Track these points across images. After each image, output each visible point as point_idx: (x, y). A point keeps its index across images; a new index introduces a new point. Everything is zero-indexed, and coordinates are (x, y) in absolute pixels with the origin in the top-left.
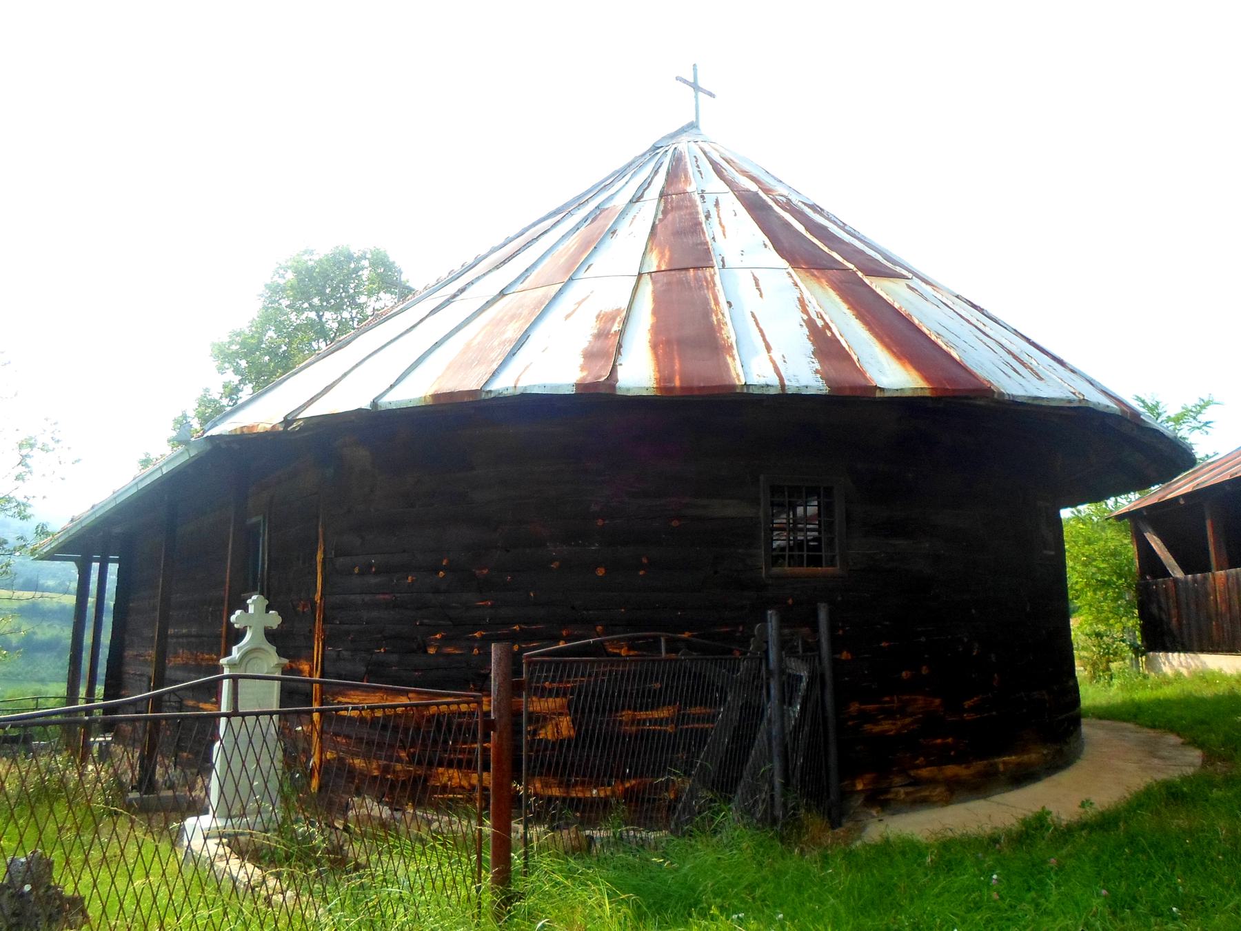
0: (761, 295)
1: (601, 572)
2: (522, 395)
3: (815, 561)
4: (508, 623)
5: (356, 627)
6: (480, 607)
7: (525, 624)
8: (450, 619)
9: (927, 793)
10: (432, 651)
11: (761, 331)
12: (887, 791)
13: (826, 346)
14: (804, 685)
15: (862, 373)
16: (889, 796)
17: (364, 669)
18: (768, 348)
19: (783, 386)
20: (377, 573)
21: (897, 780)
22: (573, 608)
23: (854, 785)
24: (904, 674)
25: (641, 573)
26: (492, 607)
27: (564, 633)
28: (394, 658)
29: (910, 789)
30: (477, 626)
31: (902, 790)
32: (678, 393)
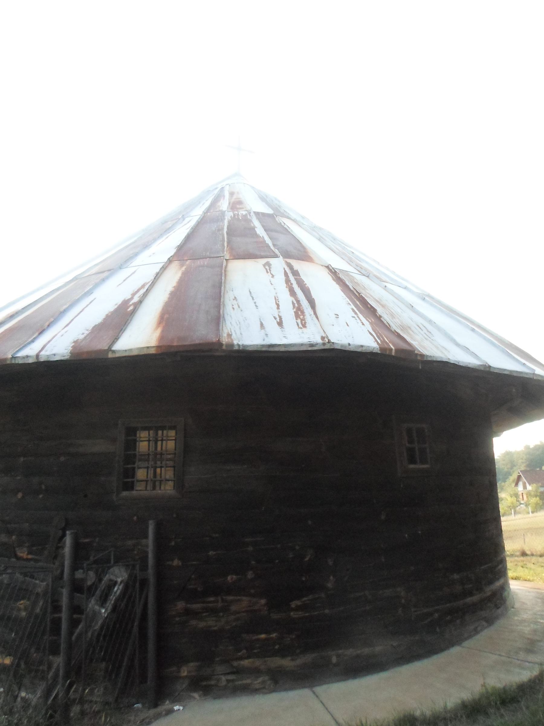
9: (248, 681)
16: (213, 683)
21: (220, 669)
23: (179, 672)
24: (229, 578)
29: (230, 677)
31: (224, 678)
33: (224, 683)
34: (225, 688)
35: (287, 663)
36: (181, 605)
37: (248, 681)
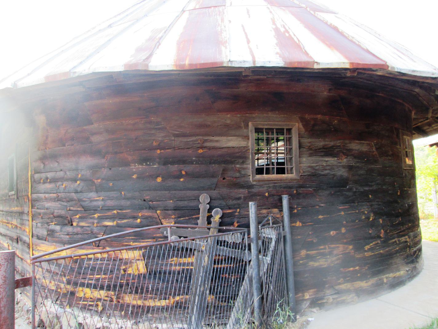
0: (249, 17)
1: (159, 180)
2: (94, 74)
3: (281, 171)
4: (110, 209)
5: (43, 211)
6: (97, 200)
7: (120, 210)
8: (83, 207)
10: (75, 224)
11: (246, 33)
12: (322, 299)
13: (284, 39)
14: (273, 243)
15: (306, 54)
16: (324, 301)
17: (45, 233)
18: (248, 42)
19: (254, 62)
20: (50, 182)
21: (328, 292)
22: (144, 200)
23: (304, 296)
24: (332, 233)
25: (182, 180)
26: (103, 200)
27: (140, 215)
28: (58, 228)
29: (335, 296)
30: (95, 210)
31: (331, 297)
32: (187, 68)
33: (331, 300)
34: (332, 303)
35: (363, 284)
36: (303, 253)
37: (344, 298)
